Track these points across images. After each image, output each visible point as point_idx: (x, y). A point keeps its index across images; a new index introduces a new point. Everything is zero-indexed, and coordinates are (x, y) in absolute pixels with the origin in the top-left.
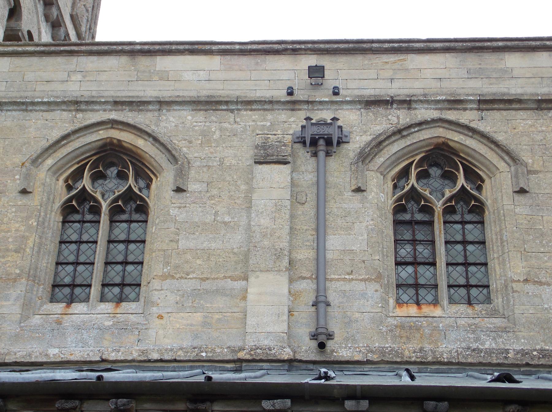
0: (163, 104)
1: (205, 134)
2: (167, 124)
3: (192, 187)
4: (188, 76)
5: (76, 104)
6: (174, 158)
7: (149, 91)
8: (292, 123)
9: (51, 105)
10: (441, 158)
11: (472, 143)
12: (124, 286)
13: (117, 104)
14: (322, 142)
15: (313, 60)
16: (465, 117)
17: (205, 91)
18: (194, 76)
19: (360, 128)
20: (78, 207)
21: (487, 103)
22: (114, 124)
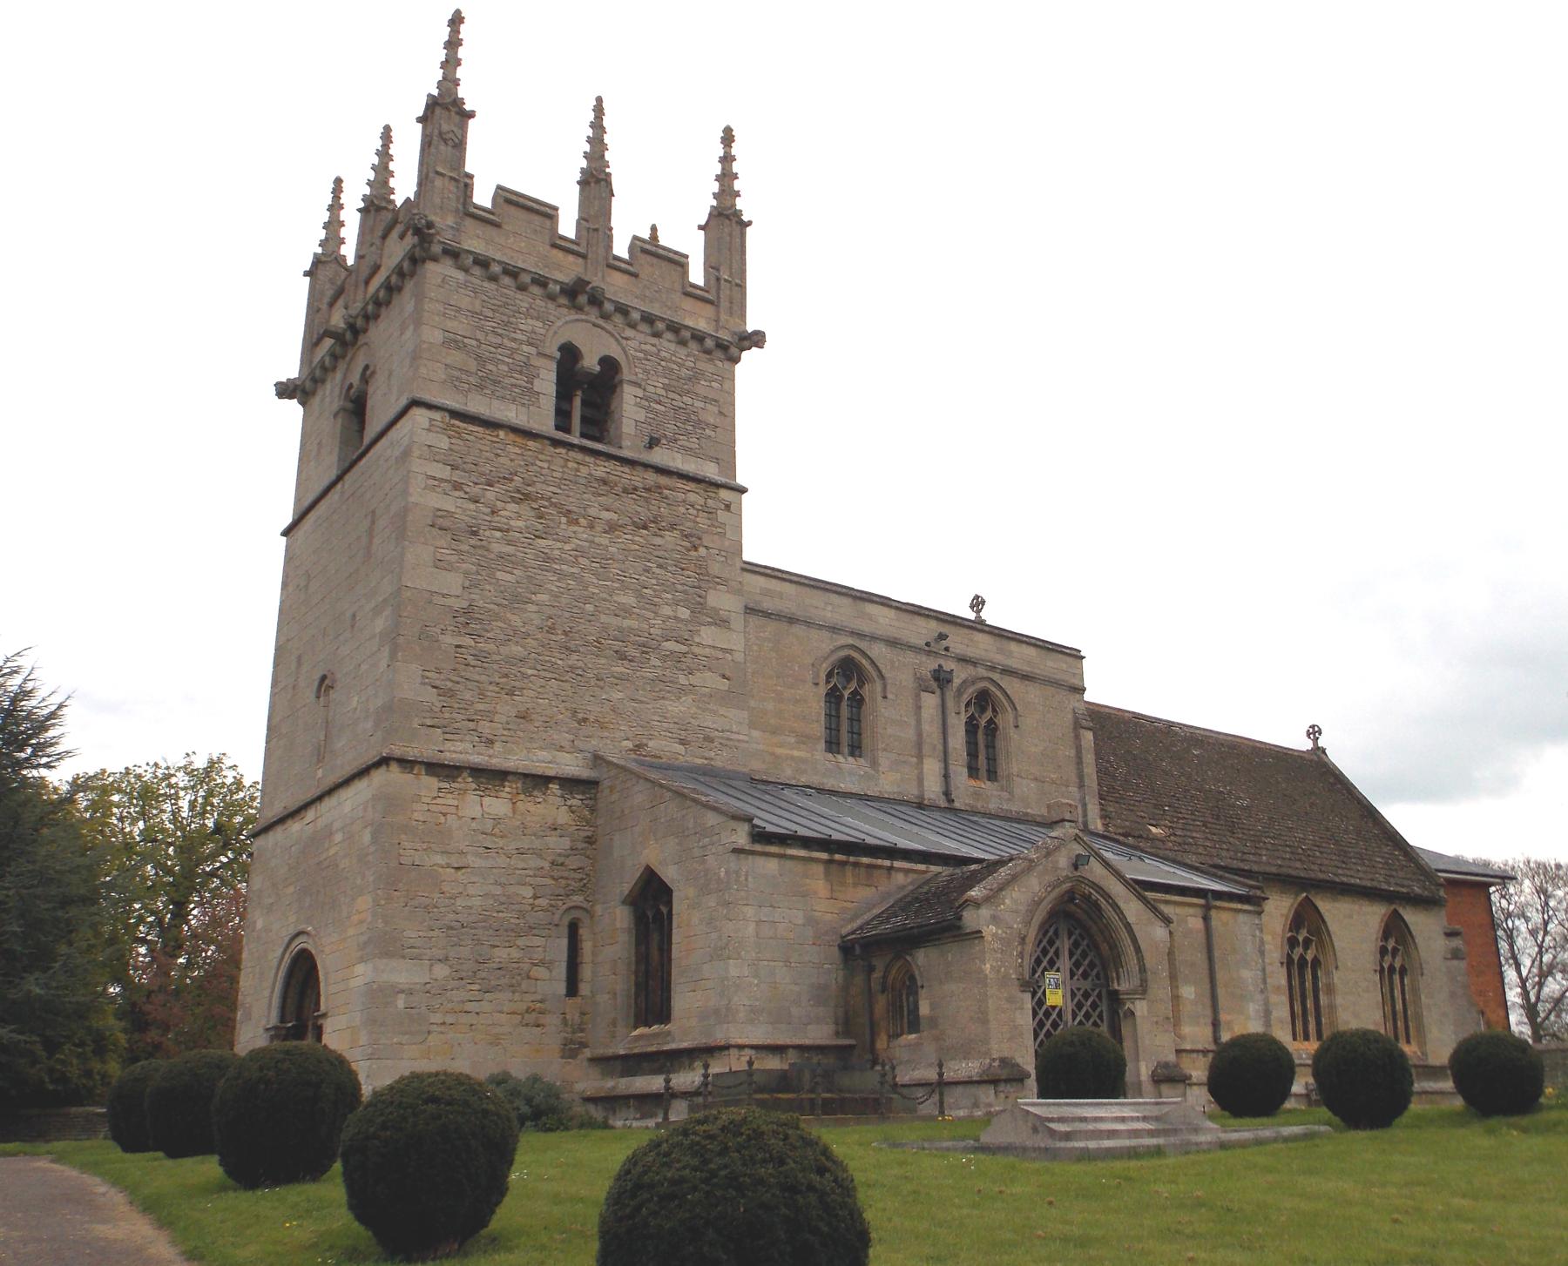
0: (874, 638)
1: (892, 662)
2: (878, 651)
3: (890, 696)
4: (881, 620)
5: (834, 629)
6: (882, 677)
7: (865, 627)
8: (931, 664)
9: (821, 627)
10: (983, 700)
11: (998, 693)
12: (856, 749)
13: (853, 633)
14: (941, 679)
15: (934, 627)
16: (996, 676)
17: (893, 633)
18: (885, 621)
19: (960, 674)
20: (833, 696)
21: (1007, 671)
22: (852, 647)
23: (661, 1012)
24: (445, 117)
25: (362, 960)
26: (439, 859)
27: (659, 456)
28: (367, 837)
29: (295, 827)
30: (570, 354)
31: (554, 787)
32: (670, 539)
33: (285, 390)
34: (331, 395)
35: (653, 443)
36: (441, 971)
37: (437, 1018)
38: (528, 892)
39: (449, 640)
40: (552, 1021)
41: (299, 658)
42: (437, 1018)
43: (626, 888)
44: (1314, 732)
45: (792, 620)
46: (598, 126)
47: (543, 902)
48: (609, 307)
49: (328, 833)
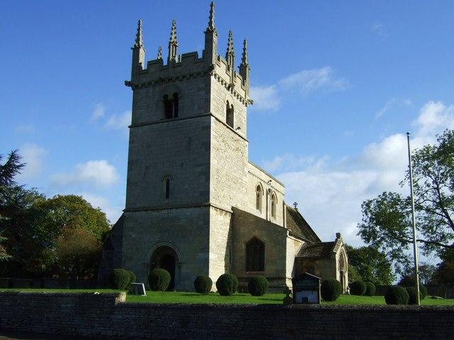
23: (261, 268)
25: (202, 252)
27: (238, 131)
29: (155, 213)
31: (224, 213)
33: (127, 84)
35: (239, 128)
41: (147, 168)
44: (295, 204)
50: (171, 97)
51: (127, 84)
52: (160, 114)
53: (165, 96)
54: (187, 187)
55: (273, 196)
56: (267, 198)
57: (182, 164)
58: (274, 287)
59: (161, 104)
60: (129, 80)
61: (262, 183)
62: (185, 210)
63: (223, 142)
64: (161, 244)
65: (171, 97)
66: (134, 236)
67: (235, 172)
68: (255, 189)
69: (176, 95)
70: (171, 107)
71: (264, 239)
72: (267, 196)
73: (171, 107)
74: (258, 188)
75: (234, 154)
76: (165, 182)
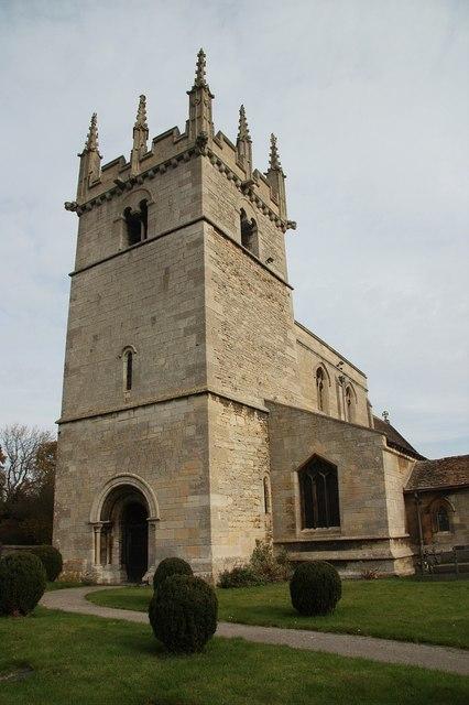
23: (335, 520)
24: (199, 94)
25: (196, 493)
26: (226, 445)
27: (269, 266)
28: (191, 431)
29: (107, 422)
30: (243, 214)
31: (245, 411)
32: (276, 305)
33: (70, 207)
34: (114, 210)
35: (270, 260)
36: (230, 500)
37: (230, 524)
38: (252, 463)
39: (221, 336)
40: (262, 525)
41: (95, 337)
42: (230, 524)
43: (298, 464)
44: (385, 414)
45: (308, 348)
46: (242, 119)
47: (256, 468)
48: (254, 197)
49: (147, 426)
50: (136, 208)
51: (70, 207)
52: (121, 242)
53: (127, 211)
54: (162, 361)
55: (348, 389)
56: (338, 392)
57: (154, 319)
58: (364, 560)
59: (121, 227)
60: (72, 198)
61: (327, 365)
62: (159, 408)
63: (237, 274)
64: (116, 483)
65: (136, 208)
66: (72, 469)
67: (267, 335)
68: (314, 374)
69: (144, 205)
70: (136, 226)
71: (334, 458)
72: (337, 388)
73: (136, 226)
74: (320, 373)
75: (264, 303)
76: (125, 359)
